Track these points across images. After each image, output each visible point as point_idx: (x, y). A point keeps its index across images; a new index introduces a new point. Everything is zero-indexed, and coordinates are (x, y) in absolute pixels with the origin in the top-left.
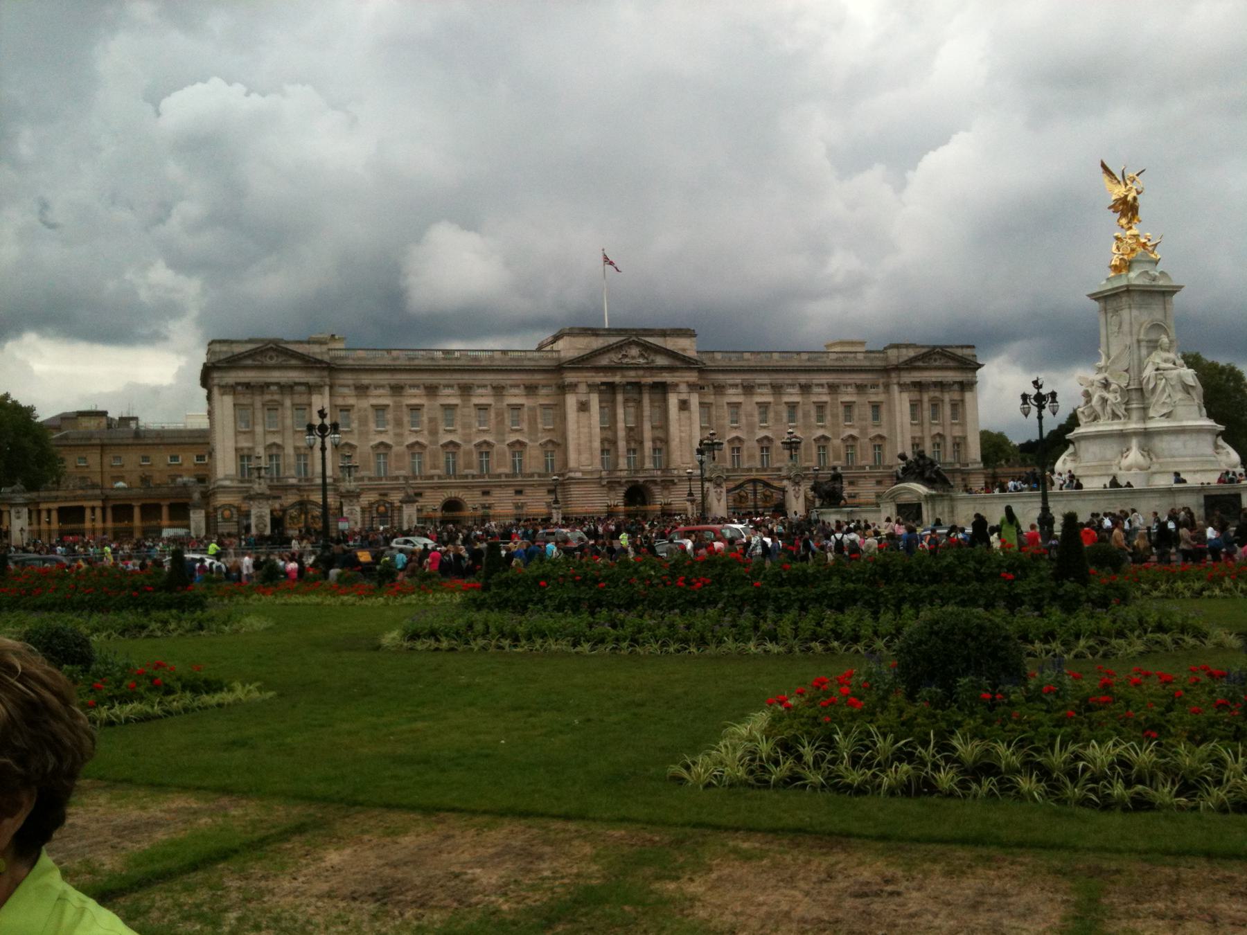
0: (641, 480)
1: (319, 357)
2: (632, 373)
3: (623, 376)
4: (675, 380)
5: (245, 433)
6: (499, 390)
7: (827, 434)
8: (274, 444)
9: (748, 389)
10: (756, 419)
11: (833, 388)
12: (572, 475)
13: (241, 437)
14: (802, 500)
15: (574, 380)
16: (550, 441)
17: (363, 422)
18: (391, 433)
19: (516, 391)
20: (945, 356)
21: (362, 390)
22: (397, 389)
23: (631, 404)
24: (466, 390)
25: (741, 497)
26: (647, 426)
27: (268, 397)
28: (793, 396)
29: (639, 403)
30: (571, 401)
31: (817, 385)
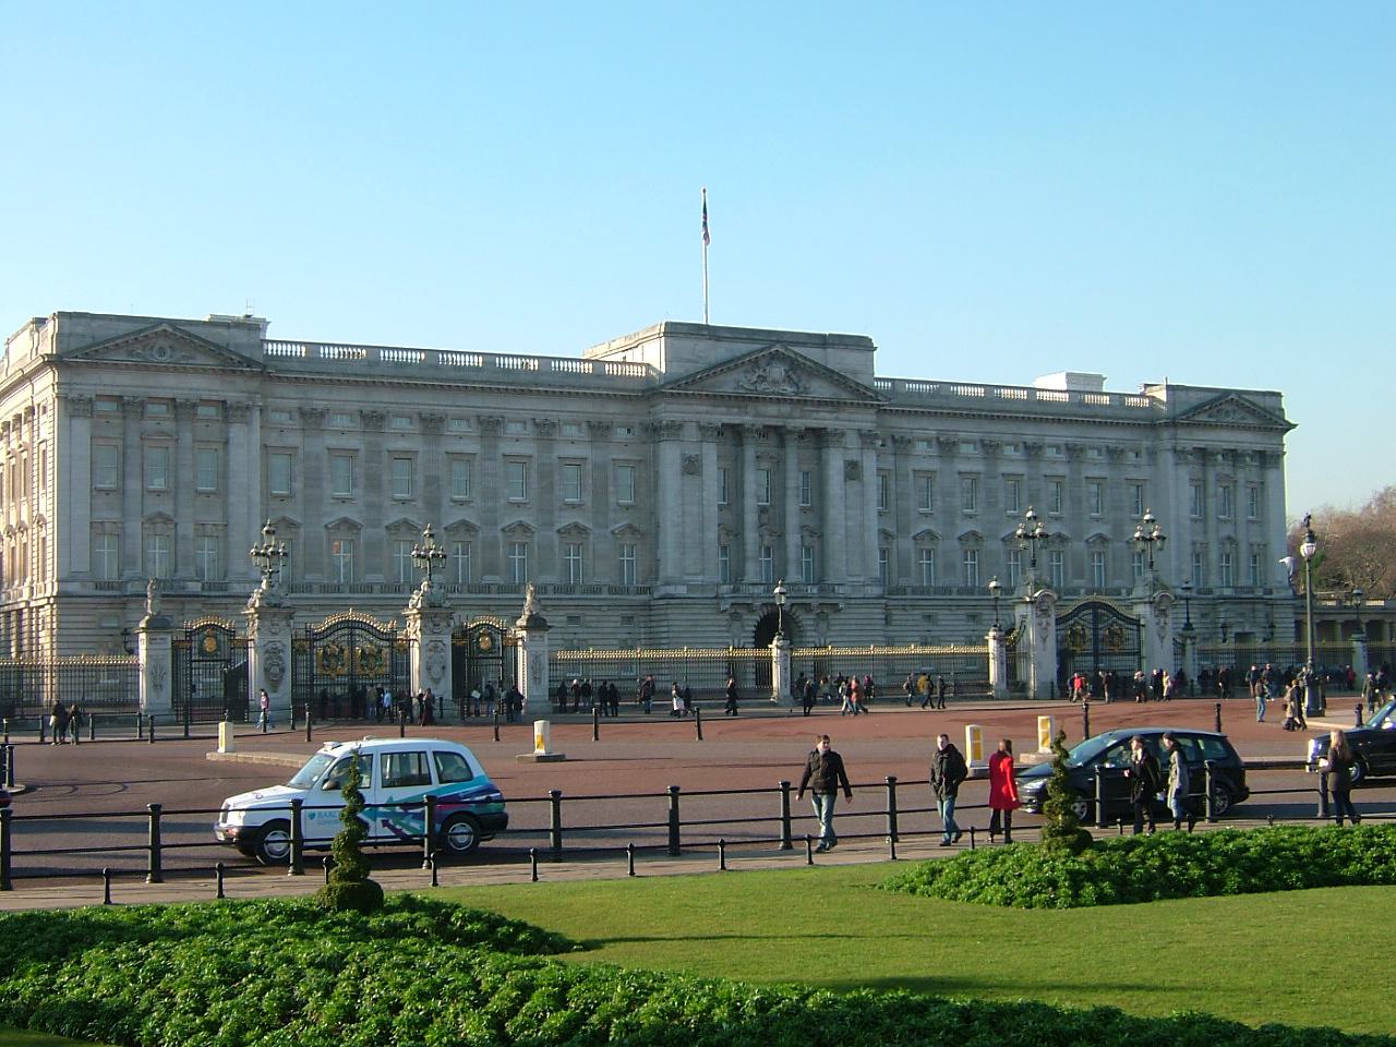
2: (772, 409)
3: (757, 415)
4: (838, 425)
5: (107, 492)
6: (545, 430)
8: (160, 514)
9: (947, 448)
11: (1074, 452)
12: (671, 590)
14: (1168, 642)
15: (677, 417)
16: (630, 527)
17: (314, 479)
20: (1243, 407)
21: (312, 419)
22: (373, 420)
24: (490, 426)
25: (1074, 633)
26: (793, 505)
28: (1012, 462)
29: (779, 463)
30: (670, 456)
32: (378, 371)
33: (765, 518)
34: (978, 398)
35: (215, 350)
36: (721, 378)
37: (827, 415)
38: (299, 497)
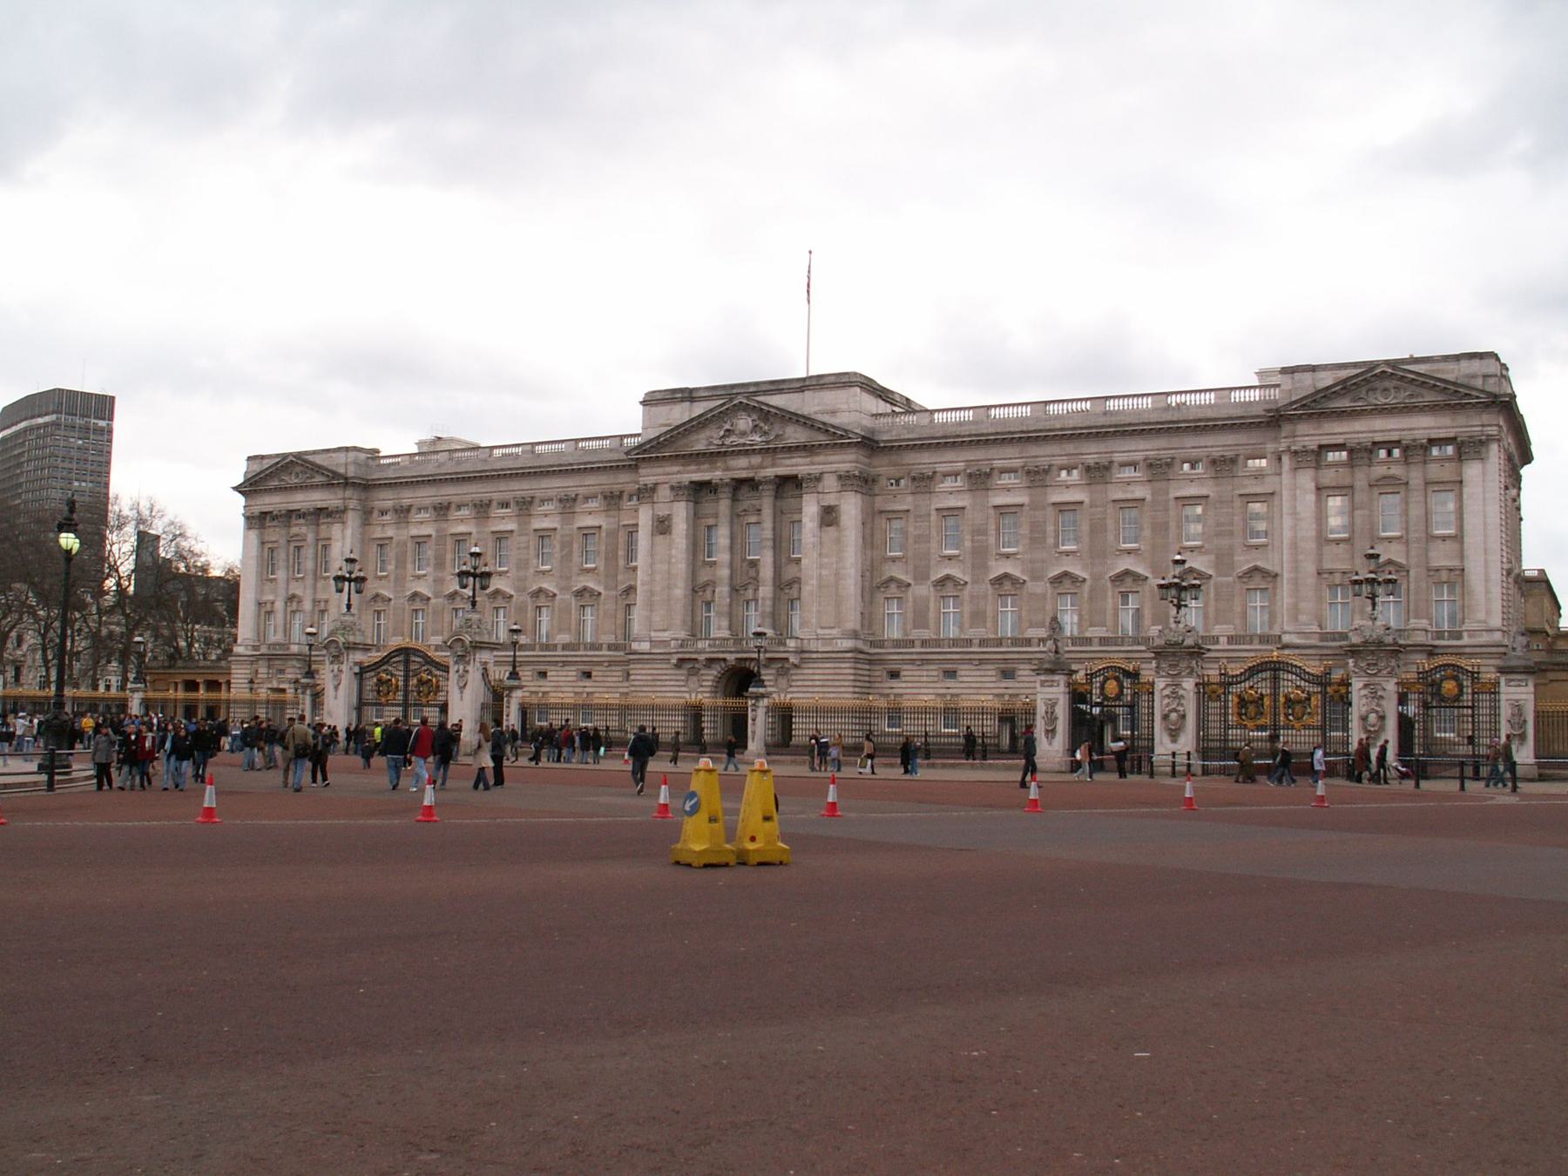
0: (731, 657)
1: (342, 471)
2: (742, 462)
3: (728, 469)
4: (815, 469)
6: (568, 503)
7: (1140, 570)
9: (980, 480)
10: (992, 540)
11: (1159, 469)
13: (268, 586)
15: (650, 480)
17: (401, 563)
18: (430, 579)
19: (593, 505)
23: (753, 519)
27: (295, 530)
28: (1069, 487)
31: (1123, 465)
32: (443, 471)
33: (752, 573)
34: (1022, 420)
35: (318, 469)
36: (694, 437)
37: (800, 460)
38: (392, 577)
